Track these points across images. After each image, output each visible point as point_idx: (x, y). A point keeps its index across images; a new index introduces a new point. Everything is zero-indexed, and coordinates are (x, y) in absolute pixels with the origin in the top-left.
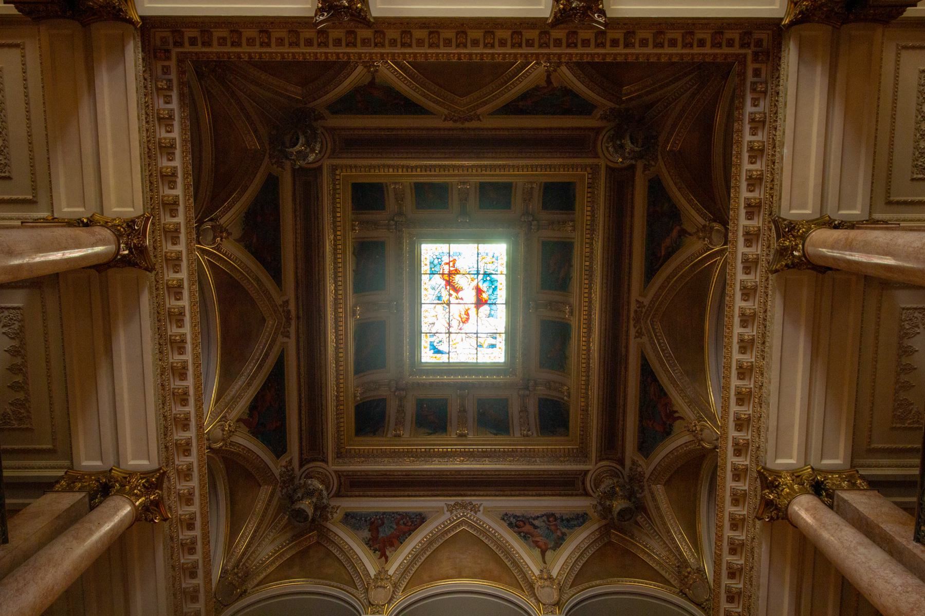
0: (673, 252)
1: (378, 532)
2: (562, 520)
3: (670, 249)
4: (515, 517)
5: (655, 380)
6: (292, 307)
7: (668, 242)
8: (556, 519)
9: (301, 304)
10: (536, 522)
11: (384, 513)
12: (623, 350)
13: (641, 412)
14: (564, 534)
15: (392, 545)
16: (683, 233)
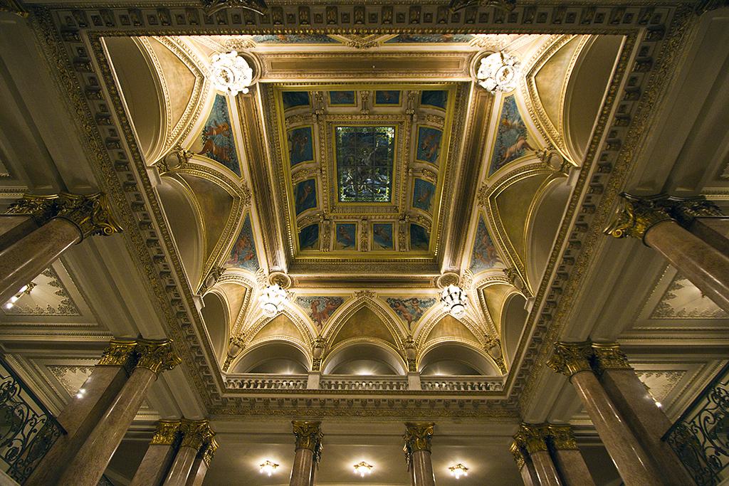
0: (516, 157)
1: (316, 309)
2: (421, 303)
3: (513, 155)
4: (394, 300)
5: (487, 233)
6: (250, 186)
7: (512, 149)
8: (418, 302)
9: (256, 185)
10: (406, 304)
11: (319, 297)
12: (469, 212)
13: (474, 251)
14: (422, 311)
15: (324, 318)
16: (525, 146)
